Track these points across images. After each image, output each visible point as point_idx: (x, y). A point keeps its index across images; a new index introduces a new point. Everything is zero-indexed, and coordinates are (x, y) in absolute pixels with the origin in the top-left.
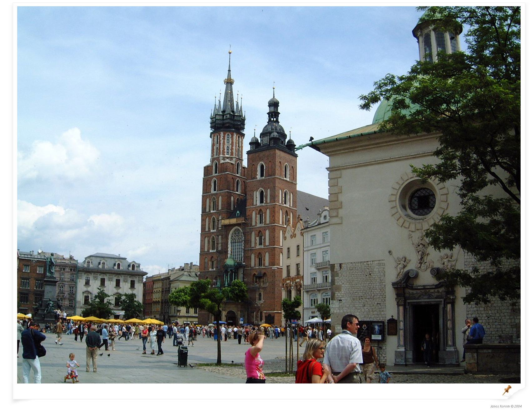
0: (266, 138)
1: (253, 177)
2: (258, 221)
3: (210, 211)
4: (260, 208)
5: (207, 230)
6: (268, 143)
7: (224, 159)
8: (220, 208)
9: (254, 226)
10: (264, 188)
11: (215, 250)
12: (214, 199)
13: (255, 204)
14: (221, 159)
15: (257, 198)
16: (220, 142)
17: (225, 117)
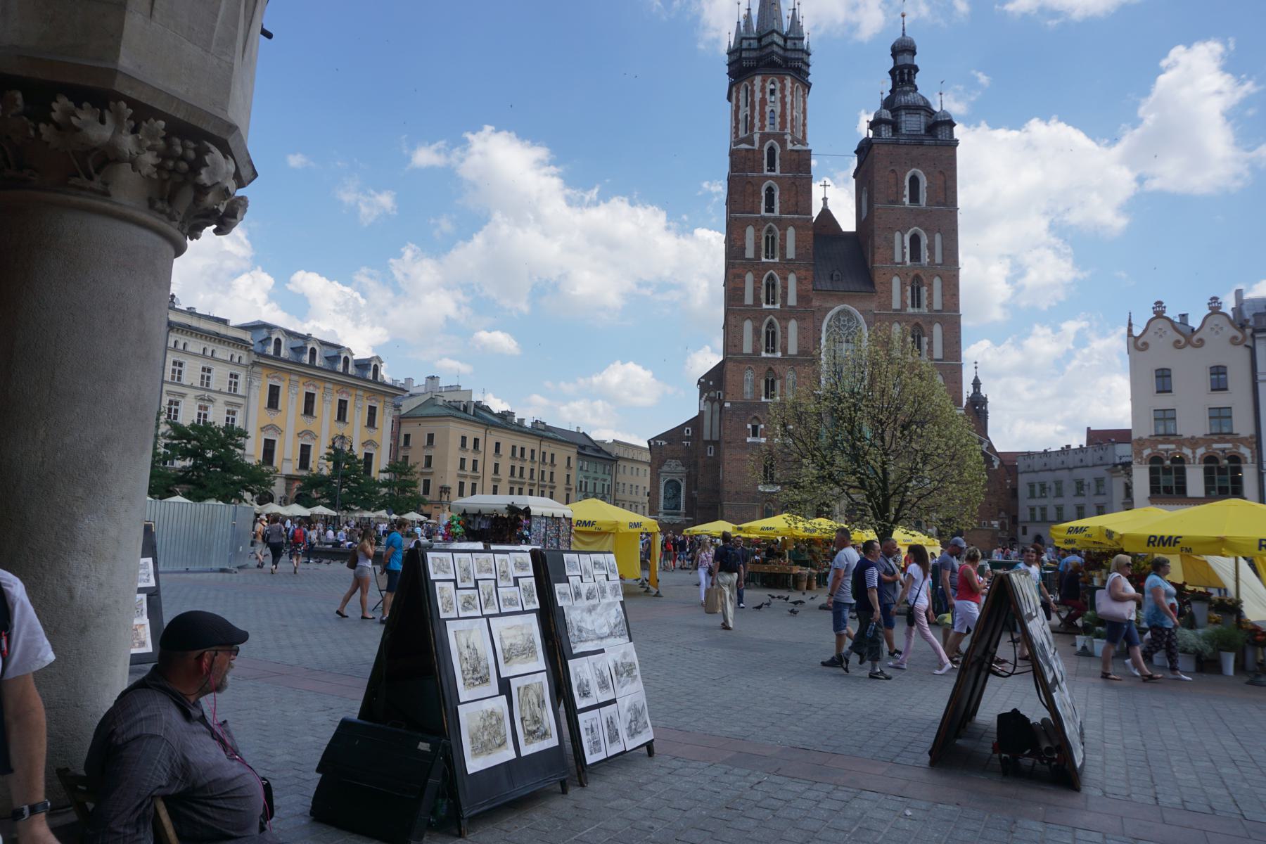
0: (914, 119)
1: (892, 198)
2: (909, 302)
3: (758, 256)
4: (918, 271)
5: (749, 300)
6: (923, 132)
7: (792, 142)
8: (791, 254)
9: (900, 310)
10: (926, 230)
11: (779, 355)
12: (770, 230)
13: (898, 258)
14: (788, 141)
15: (905, 248)
16: (783, 98)
17: (789, 44)
